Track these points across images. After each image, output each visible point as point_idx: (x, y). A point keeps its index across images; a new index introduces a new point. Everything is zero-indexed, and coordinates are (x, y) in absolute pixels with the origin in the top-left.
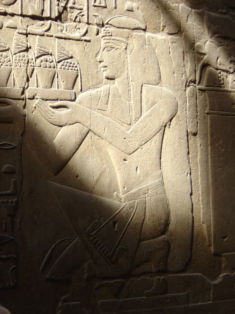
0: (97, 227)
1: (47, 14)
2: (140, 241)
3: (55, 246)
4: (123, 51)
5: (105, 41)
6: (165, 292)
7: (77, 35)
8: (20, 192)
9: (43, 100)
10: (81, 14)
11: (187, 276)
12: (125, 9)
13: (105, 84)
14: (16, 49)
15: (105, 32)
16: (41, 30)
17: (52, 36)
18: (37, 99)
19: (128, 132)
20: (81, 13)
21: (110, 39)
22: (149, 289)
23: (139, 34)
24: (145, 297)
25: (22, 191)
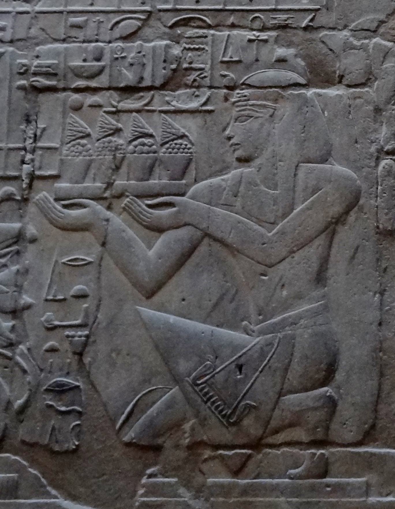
0: (208, 372)
1: (147, 83)
2: (281, 394)
3: (141, 397)
4: (266, 120)
5: (238, 109)
6: (324, 474)
7: (194, 105)
8: (94, 322)
9: (137, 197)
10: (202, 76)
11: (366, 452)
12: (274, 60)
13: (236, 168)
14: (100, 134)
15: (239, 95)
16: (138, 105)
17: (153, 111)
18: (128, 196)
19: (270, 234)
20: (201, 74)
21: (246, 105)
22: (295, 468)
23: (296, 92)
24: (287, 480)
25: (97, 321)
